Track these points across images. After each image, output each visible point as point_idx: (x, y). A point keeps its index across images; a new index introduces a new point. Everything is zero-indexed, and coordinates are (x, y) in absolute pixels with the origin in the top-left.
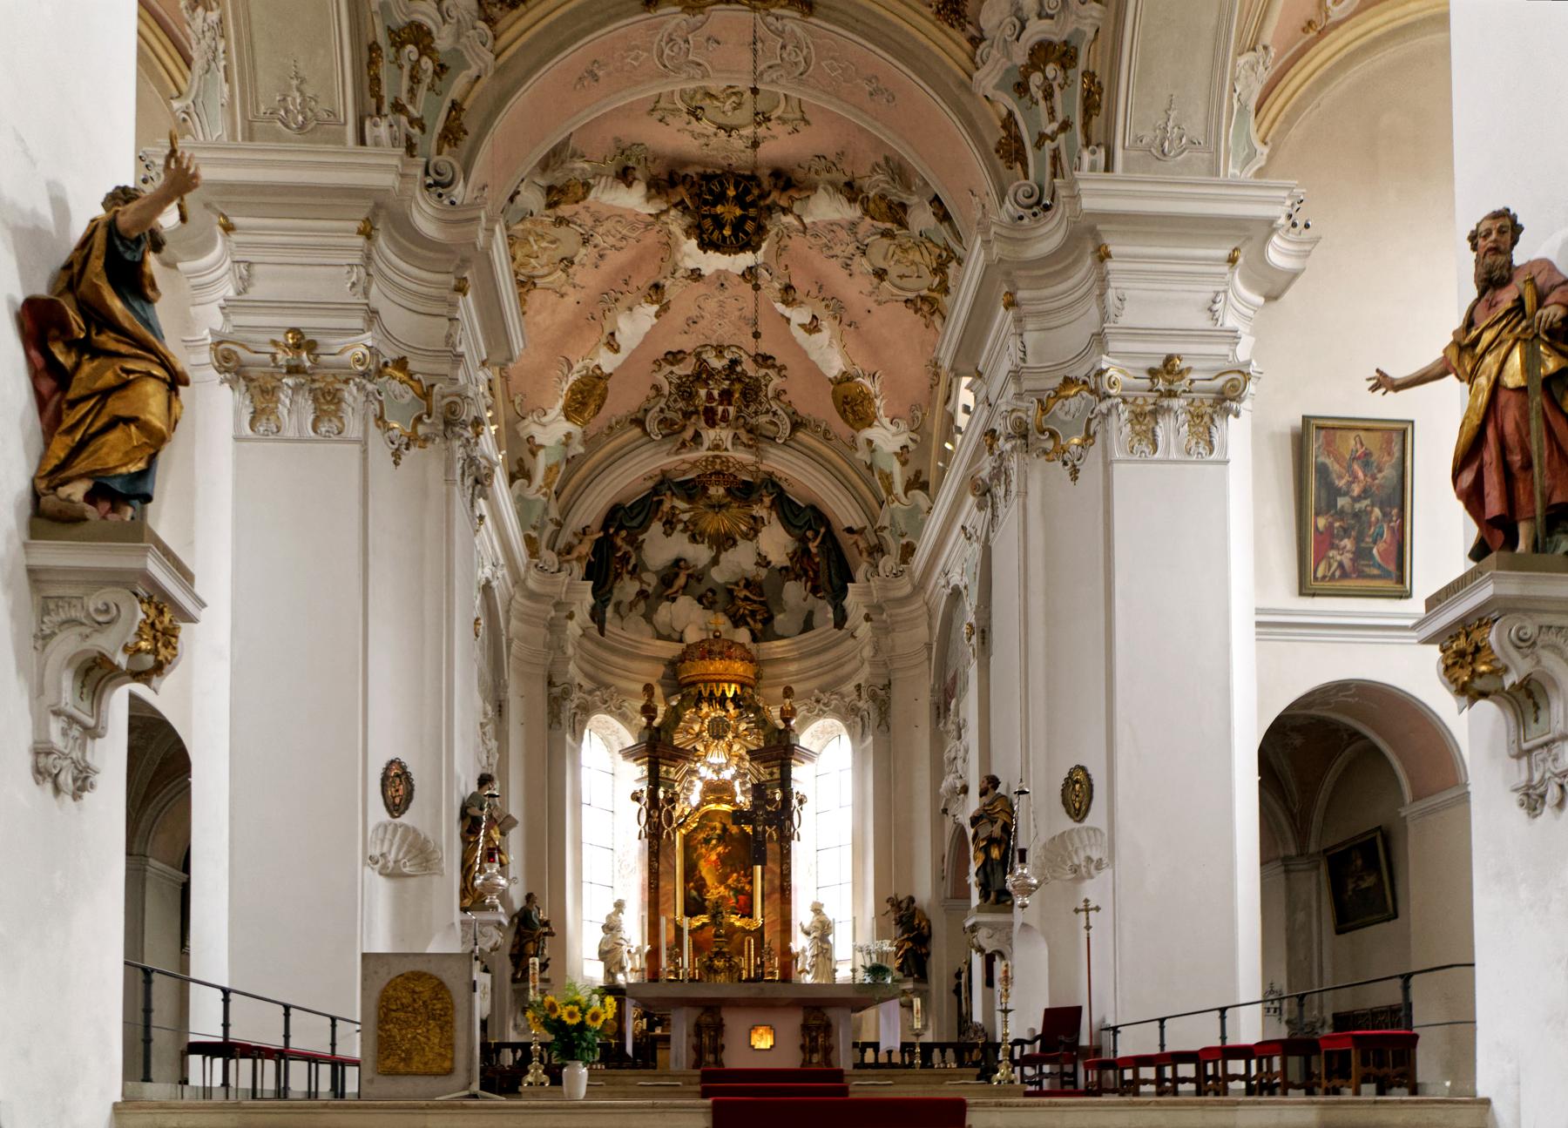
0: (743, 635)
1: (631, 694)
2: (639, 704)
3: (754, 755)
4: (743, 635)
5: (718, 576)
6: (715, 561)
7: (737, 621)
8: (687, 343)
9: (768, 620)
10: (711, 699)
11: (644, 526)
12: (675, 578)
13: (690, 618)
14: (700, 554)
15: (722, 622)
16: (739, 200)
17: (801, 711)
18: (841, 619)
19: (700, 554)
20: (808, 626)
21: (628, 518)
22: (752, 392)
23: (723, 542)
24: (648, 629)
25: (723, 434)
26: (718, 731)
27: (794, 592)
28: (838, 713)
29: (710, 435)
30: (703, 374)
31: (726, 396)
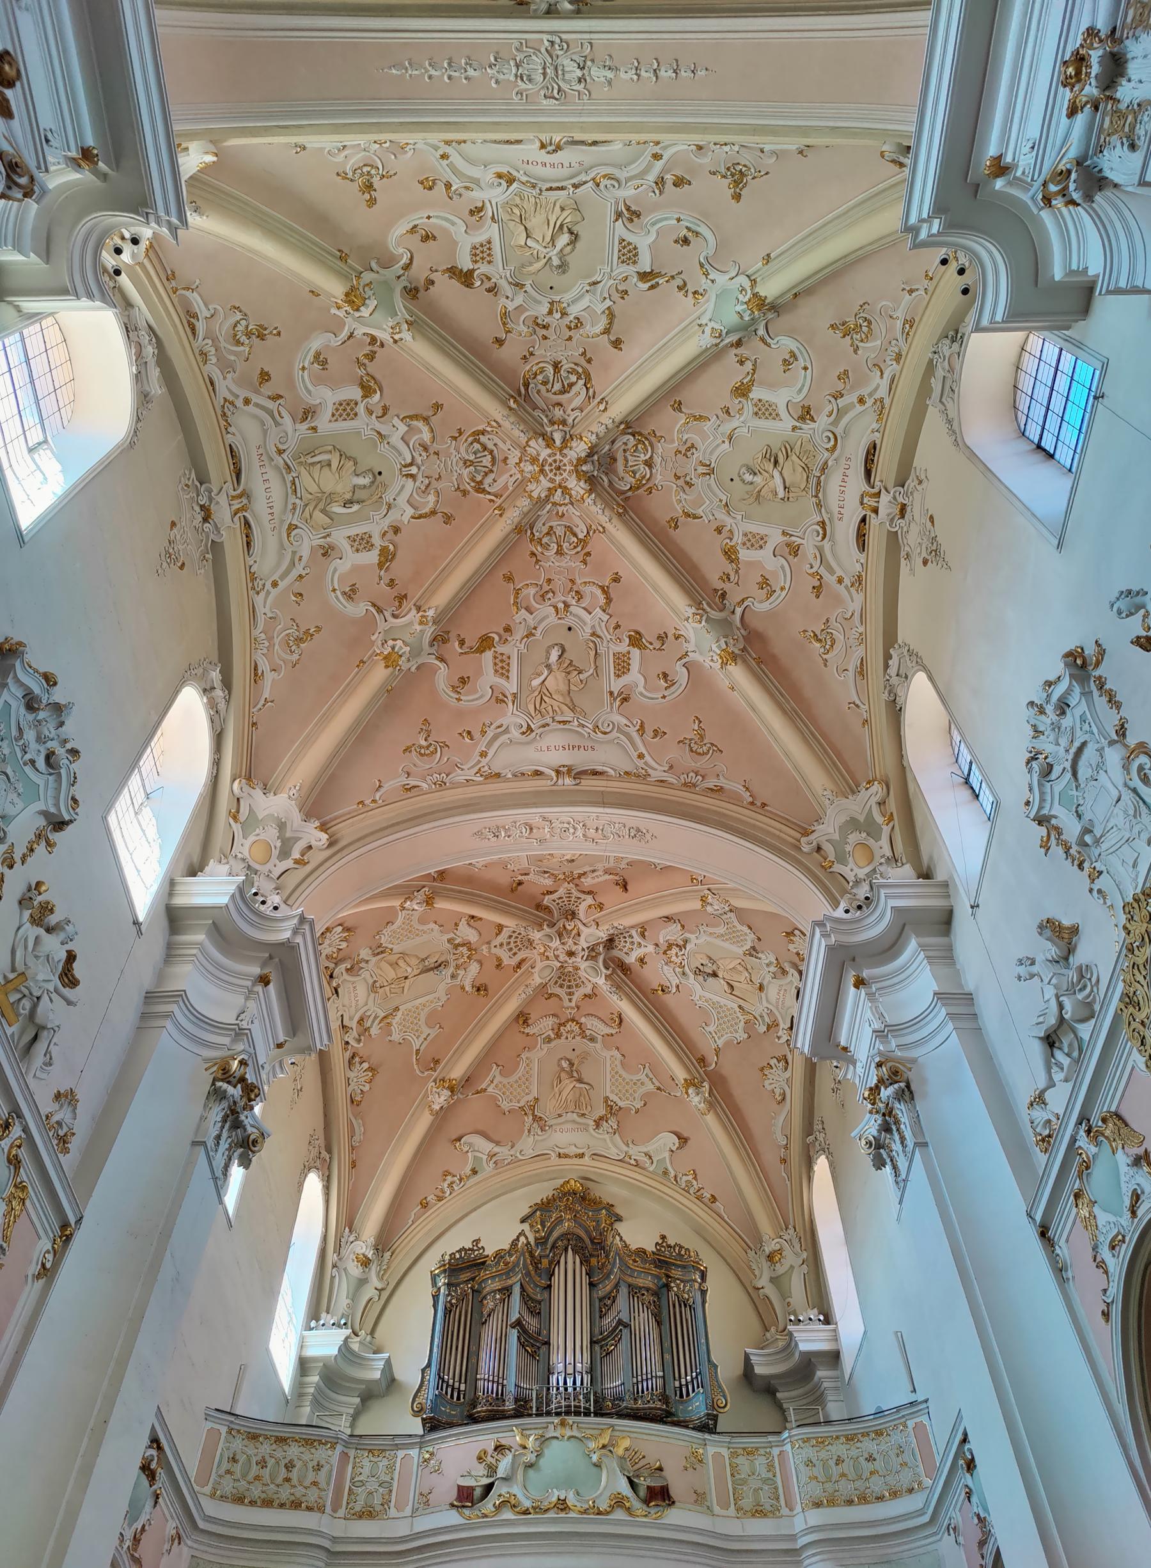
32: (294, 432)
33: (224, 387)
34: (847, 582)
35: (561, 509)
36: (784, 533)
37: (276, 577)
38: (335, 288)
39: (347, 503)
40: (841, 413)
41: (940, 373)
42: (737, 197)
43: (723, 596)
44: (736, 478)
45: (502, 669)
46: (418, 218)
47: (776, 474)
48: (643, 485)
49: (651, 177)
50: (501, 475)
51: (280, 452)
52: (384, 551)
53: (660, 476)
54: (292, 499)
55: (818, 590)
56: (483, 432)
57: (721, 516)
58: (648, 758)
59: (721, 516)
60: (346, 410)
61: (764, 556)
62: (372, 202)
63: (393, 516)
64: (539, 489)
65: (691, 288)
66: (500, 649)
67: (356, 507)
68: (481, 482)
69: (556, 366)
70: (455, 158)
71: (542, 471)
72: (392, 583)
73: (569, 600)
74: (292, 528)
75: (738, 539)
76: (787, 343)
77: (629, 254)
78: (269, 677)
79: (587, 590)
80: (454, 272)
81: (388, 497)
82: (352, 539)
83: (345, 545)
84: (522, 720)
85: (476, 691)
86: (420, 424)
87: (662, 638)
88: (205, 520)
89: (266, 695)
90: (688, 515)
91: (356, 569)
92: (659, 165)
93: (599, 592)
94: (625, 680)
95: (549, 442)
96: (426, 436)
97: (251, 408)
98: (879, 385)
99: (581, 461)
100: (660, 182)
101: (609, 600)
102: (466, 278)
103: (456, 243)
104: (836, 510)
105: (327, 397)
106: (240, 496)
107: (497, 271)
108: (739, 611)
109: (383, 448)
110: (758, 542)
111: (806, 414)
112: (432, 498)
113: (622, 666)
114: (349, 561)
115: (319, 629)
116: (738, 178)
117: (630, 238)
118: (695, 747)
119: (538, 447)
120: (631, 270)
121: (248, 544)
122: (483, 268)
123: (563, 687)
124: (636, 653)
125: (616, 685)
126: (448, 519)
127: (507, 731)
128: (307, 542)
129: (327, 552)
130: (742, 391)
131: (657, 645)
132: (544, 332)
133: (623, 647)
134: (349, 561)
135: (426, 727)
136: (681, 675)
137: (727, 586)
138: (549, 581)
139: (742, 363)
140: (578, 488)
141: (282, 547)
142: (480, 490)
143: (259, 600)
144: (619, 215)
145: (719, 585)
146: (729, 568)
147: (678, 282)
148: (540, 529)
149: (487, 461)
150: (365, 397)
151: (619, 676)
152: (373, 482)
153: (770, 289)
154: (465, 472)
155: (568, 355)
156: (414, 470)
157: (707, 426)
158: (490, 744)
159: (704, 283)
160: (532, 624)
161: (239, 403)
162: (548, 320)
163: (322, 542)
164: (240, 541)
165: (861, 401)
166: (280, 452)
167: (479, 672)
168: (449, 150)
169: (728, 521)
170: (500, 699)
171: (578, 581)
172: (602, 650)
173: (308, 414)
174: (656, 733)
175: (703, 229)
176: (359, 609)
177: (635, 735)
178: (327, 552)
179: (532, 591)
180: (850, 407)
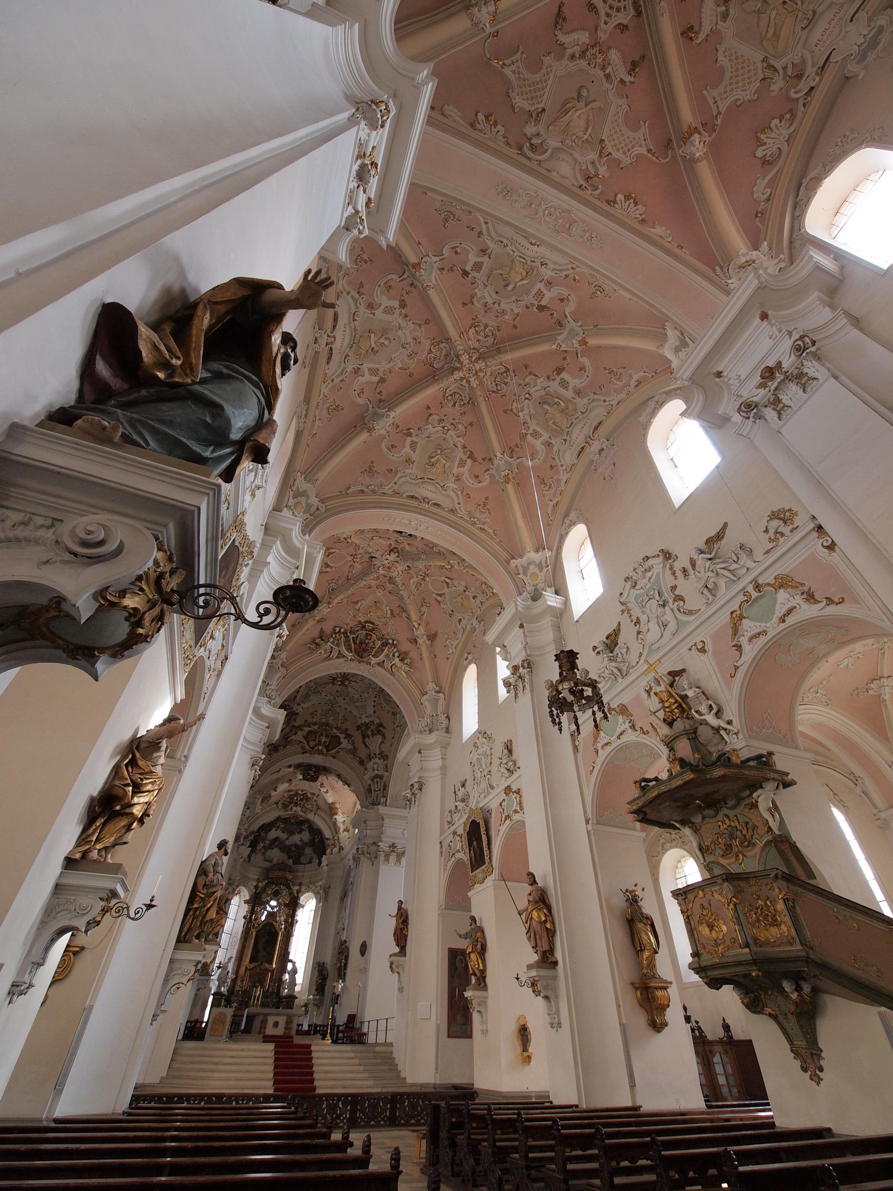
0: (290, 862)
1: (253, 880)
2: (255, 884)
3: (286, 905)
4: (290, 862)
5: (287, 843)
6: (288, 838)
7: (290, 857)
8: (294, 789)
9: (299, 857)
10: (276, 884)
11: (270, 830)
12: (275, 842)
13: (276, 855)
14: (284, 836)
15: (286, 856)
16: (315, 772)
17: (303, 889)
18: (320, 864)
19: (284, 836)
20: (310, 862)
21: (266, 828)
22: (308, 799)
23: (291, 833)
24: (262, 857)
25: (298, 809)
26: (276, 895)
27: (308, 851)
28: (313, 892)
29: (294, 809)
30: (297, 794)
31: (302, 800)
32: (557, 443)
33: (564, 477)
34: (345, 293)
35: (476, 345)
36: (374, 314)
37: (602, 403)
38: (510, 487)
39: (557, 404)
40: (341, 374)
41: (303, 416)
42: (372, 462)
43: (412, 285)
44: (392, 339)
45: (540, 295)
46: (477, 485)
47: (373, 345)
48: (435, 343)
49: (399, 474)
50: (495, 371)
51: (565, 440)
52: (558, 374)
53: (427, 344)
54: (574, 422)
55: (361, 285)
56: (494, 392)
57: (403, 324)
58: (482, 221)
59: (403, 324)
60: (536, 435)
61: (385, 302)
62: (487, 498)
63: (546, 384)
64: (481, 365)
65: (395, 427)
66: (536, 303)
67: (556, 400)
68: (505, 372)
69: (454, 405)
70: (456, 501)
71: (477, 373)
72: (565, 359)
73: (491, 305)
74: (583, 413)
75: (397, 312)
76: (361, 401)
77: (413, 445)
78: (636, 377)
79: (480, 306)
80: (474, 460)
81: (543, 393)
82: (566, 388)
83: (571, 388)
84: (543, 270)
85: (559, 293)
86: (515, 411)
87: (452, 269)
88: (602, 449)
89: (642, 374)
90: (420, 325)
91: (574, 376)
92: (395, 480)
93: (476, 303)
94: (479, 260)
95: (468, 382)
96: (515, 404)
97: (563, 462)
98: (325, 390)
99: (458, 369)
100: (396, 474)
101: (472, 297)
102: (471, 456)
103: (469, 471)
104: (348, 330)
105: (538, 444)
106: (587, 442)
107: (460, 454)
108: (405, 276)
109: (532, 412)
110: (389, 310)
111: (357, 371)
112: (527, 380)
113: (478, 266)
114: (575, 382)
115: (605, 369)
116: (370, 471)
117: (411, 452)
118: (452, 216)
119: (474, 383)
120: (414, 439)
121: (600, 423)
122: (464, 457)
123: (513, 273)
124: (468, 269)
125: (485, 259)
126: (526, 367)
127: (554, 269)
128: (581, 402)
129: (578, 393)
130: (382, 380)
131: (455, 268)
132: (454, 422)
133: (473, 274)
134: (575, 382)
135: (593, 296)
136: (446, 251)
137: (408, 288)
138: (497, 316)
139: (380, 392)
140: (465, 359)
141: (591, 410)
142: (507, 370)
143: (614, 403)
144: (413, 463)
145: (412, 289)
146: (406, 298)
147: (399, 429)
148: (490, 340)
149: (498, 379)
150: (526, 434)
151: (482, 263)
152: (544, 403)
153: (364, 436)
154: (508, 380)
155: (448, 408)
156: (527, 396)
157: (401, 366)
158: (567, 269)
159: (389, 429)
160: (514, 304)
161: (564, 468)
162: (450, 427)
163: (578, 398)
164: (601, 430)
165: (333, 381)
166: (565, 440)
167: (551, 299)
168: (457, 506)
169: (400, 320)
170: (549, 284)
171: (483, 311)
172: (484, 278)
173: (548, 444)
174: (472, 229)
175: (385, 450)
176: (585, 361)
177: (485, 233)
178: (578, 393)
179: (507, 317)
180: (337, 377)
